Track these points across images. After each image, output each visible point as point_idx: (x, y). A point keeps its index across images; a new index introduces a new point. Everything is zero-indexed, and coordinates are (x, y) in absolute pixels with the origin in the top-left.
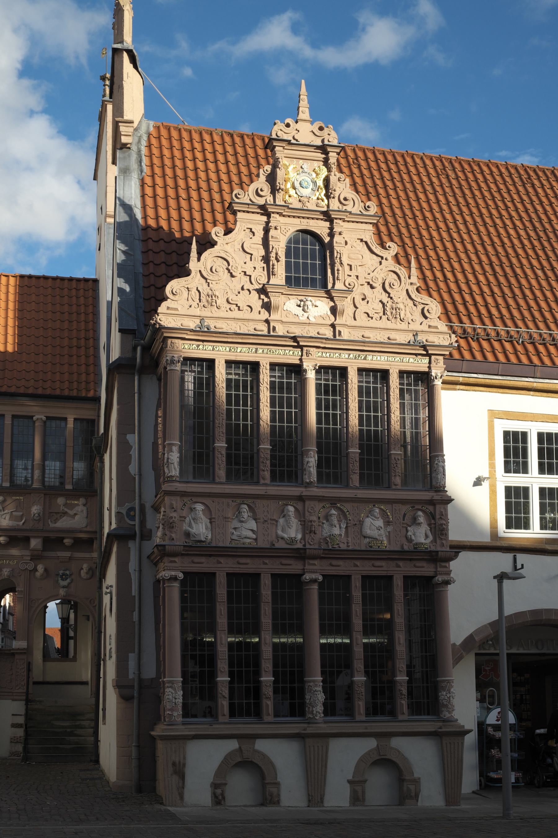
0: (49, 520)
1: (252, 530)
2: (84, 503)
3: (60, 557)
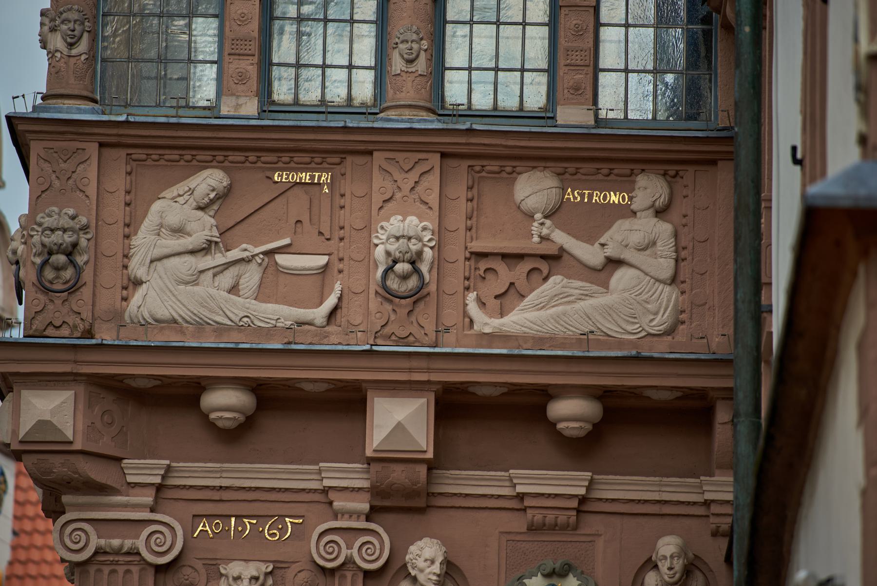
0: (472, 296)
2: (659, 203)
3: (528, 502)
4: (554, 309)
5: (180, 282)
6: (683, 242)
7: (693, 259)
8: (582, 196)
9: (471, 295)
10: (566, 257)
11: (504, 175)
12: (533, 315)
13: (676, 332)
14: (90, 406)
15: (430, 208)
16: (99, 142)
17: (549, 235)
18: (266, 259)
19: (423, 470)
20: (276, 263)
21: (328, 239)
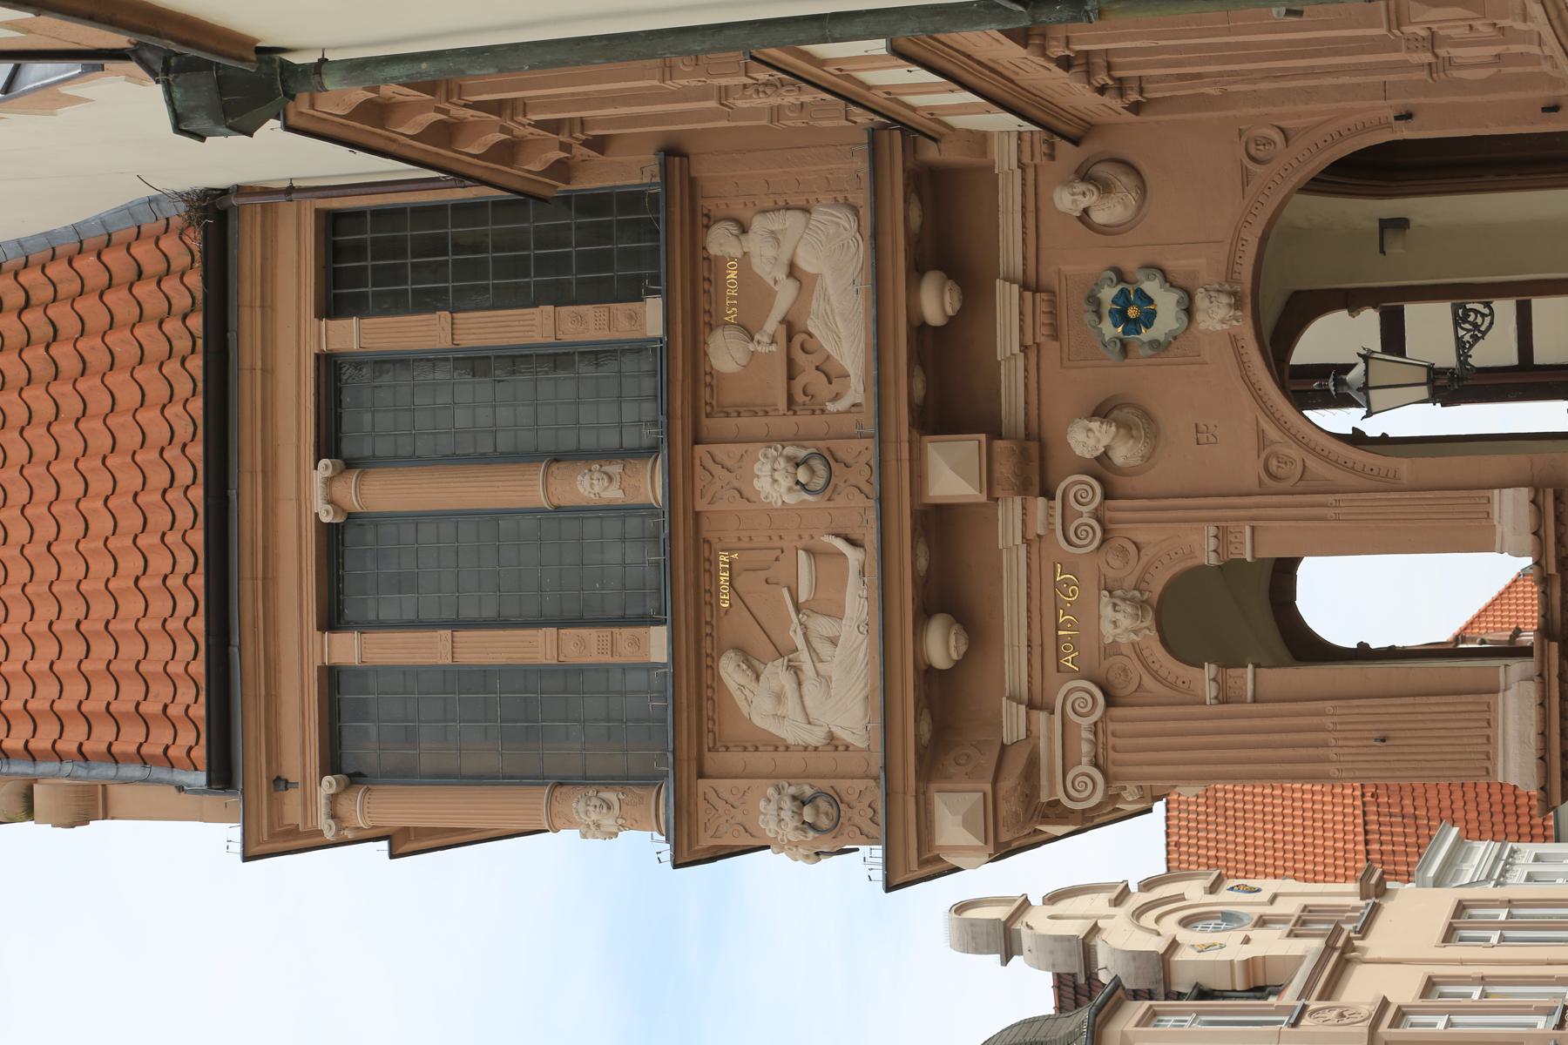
0: (830, 407)
2: (734, 229)
3: (1029, 341)
4: (840, 326)
5: (828, 694)
6: (772, 205)
7: (785, 193)
8: (731, 306)
9: (829, 408)
10: (789, 318)
11: (714, 383)
12: (846, 346)
13: (855, 204)
14: (949, 778)
15: (746, 451)
16: (697, 779)
17: (769, 335)
18: (804, 611)
19: (999, 445)
20: (807, 601)
21: (782, 552)
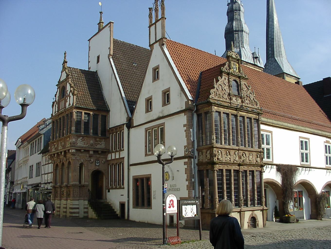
1: (229, 158)
